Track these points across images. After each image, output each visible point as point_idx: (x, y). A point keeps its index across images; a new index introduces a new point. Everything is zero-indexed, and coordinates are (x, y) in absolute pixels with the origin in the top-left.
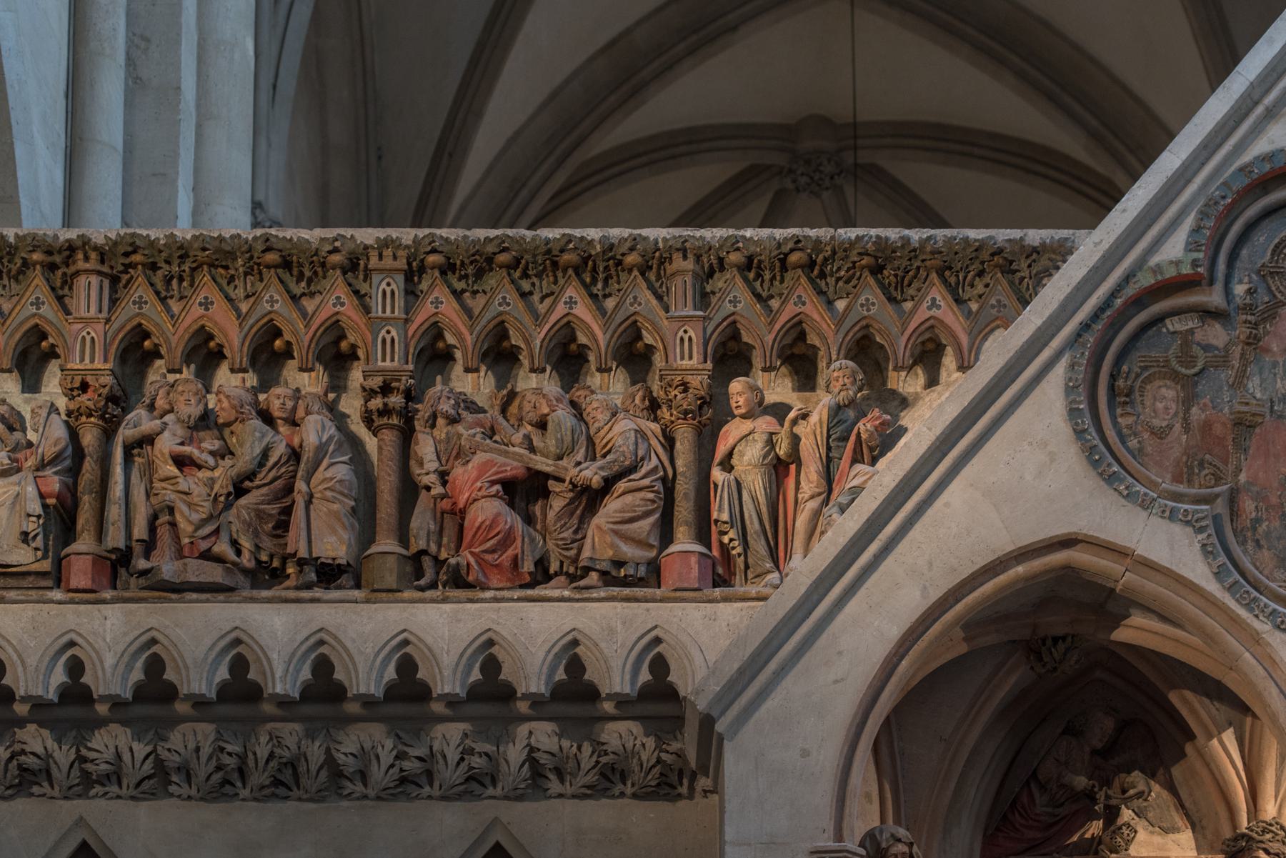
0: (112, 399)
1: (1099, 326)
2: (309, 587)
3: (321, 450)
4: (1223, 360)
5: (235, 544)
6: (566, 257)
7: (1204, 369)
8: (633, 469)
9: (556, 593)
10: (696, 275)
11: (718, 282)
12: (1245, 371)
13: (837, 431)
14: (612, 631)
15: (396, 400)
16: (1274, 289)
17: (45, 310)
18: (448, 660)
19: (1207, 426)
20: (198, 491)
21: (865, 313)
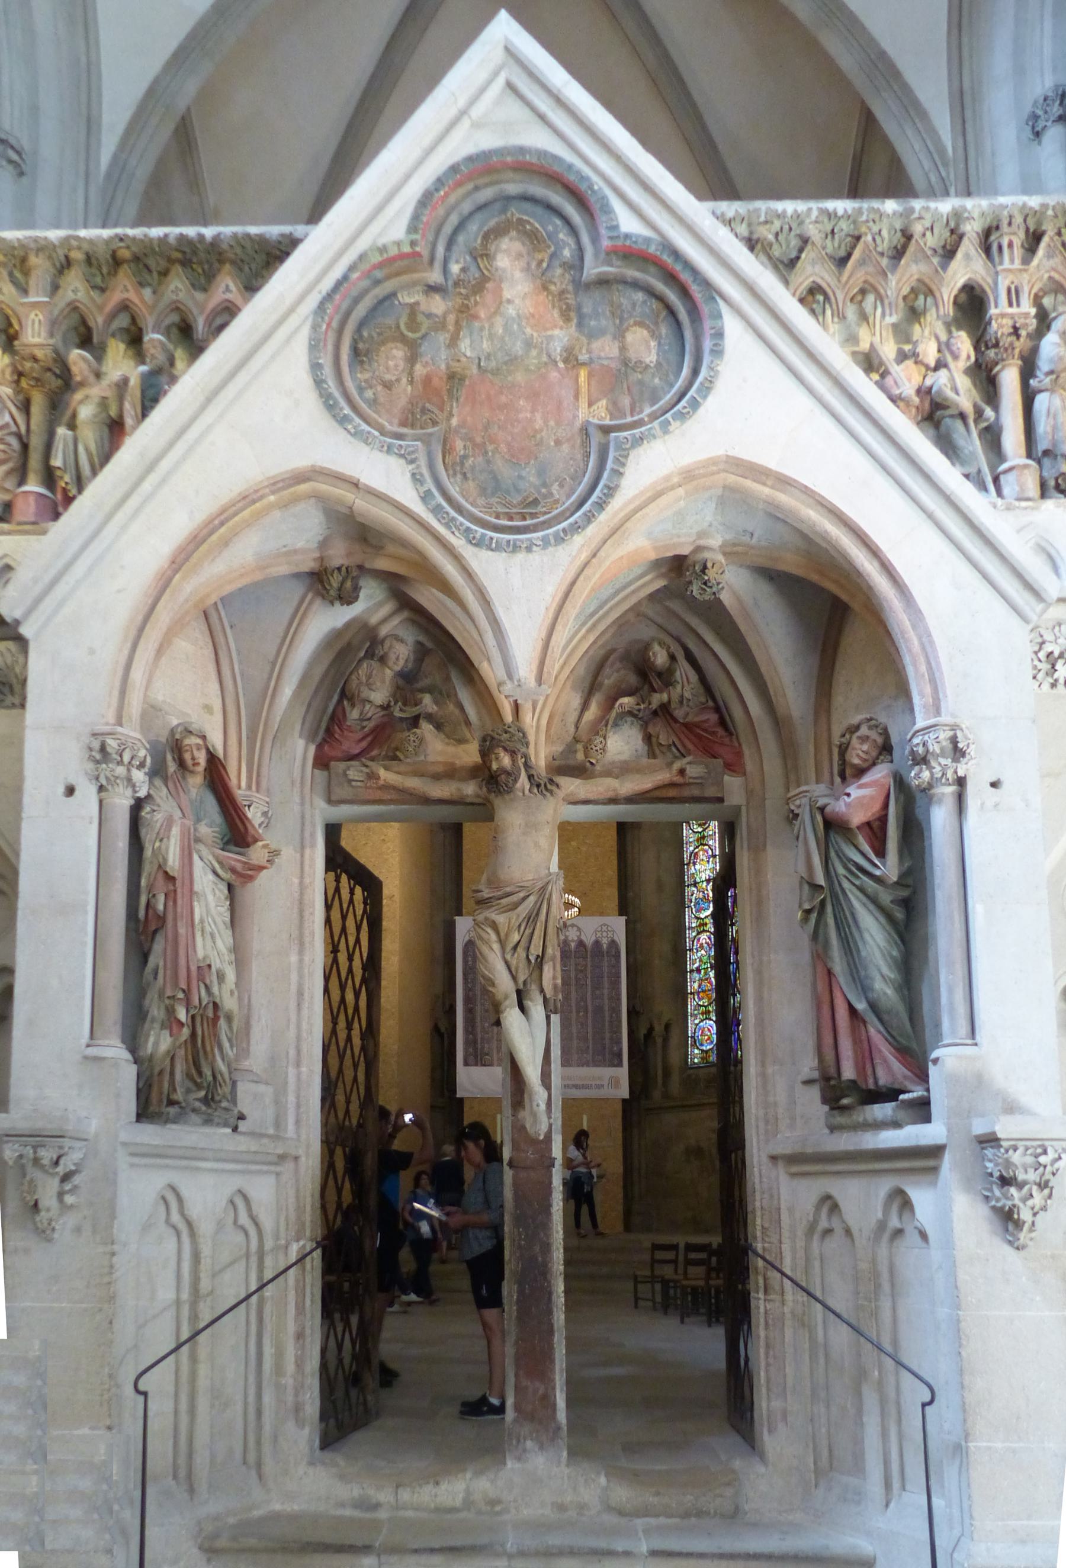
4: (442, 326)
7: (427, 334)
12: (459, 334)
16: (482, 266)
19: (427, 380)
21: (174, 297)
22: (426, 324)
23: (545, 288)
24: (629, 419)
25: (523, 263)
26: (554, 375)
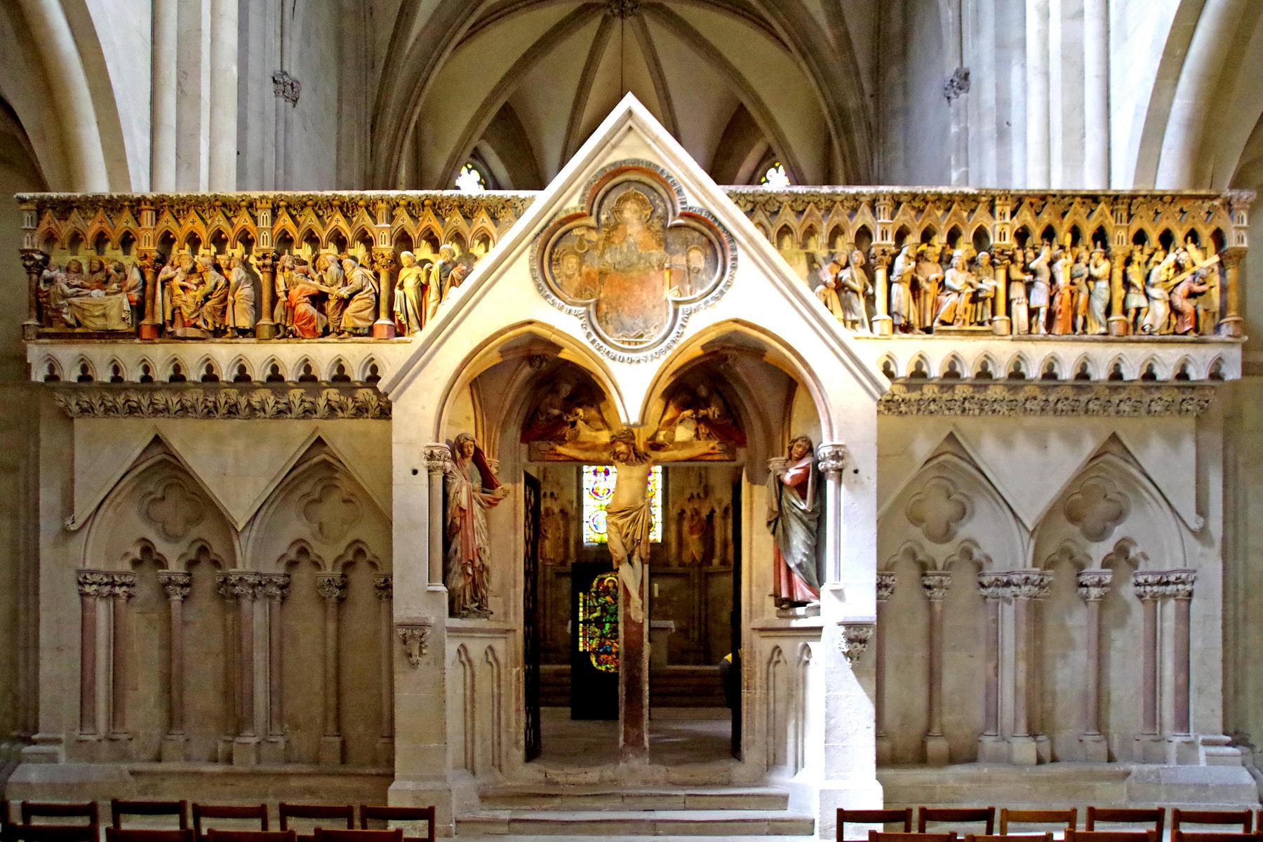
0: (157, 260)
1: (543, 235)
2: (236, 337)
3: (238, 284)
4: (595, 247)
5: (205, 321)
6: (335, 203)
8: (361, 290)
9: (331, 340)
10: (387, 210)
11: (398, 211)
13: (443, 275)
14: (354, 356)
15: (268, 261)
17: (130, 225)
18: (290, 367)
19: (588, 274)
20: (190, 300)
22: (587, 245)
23: (649, 229)
24: (689, 297)
25: (636, 216)
26: (652, 273)
